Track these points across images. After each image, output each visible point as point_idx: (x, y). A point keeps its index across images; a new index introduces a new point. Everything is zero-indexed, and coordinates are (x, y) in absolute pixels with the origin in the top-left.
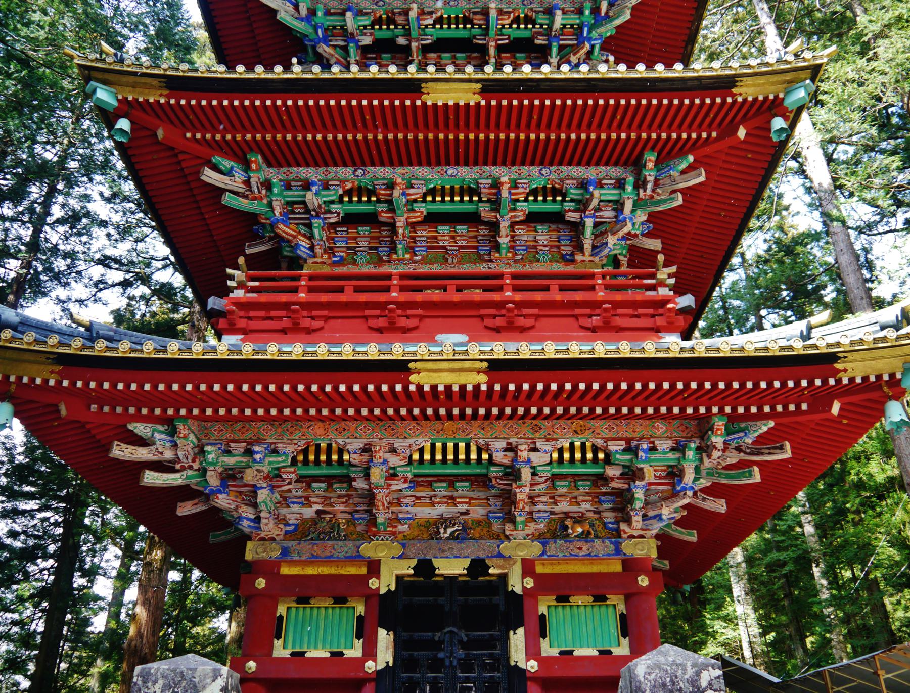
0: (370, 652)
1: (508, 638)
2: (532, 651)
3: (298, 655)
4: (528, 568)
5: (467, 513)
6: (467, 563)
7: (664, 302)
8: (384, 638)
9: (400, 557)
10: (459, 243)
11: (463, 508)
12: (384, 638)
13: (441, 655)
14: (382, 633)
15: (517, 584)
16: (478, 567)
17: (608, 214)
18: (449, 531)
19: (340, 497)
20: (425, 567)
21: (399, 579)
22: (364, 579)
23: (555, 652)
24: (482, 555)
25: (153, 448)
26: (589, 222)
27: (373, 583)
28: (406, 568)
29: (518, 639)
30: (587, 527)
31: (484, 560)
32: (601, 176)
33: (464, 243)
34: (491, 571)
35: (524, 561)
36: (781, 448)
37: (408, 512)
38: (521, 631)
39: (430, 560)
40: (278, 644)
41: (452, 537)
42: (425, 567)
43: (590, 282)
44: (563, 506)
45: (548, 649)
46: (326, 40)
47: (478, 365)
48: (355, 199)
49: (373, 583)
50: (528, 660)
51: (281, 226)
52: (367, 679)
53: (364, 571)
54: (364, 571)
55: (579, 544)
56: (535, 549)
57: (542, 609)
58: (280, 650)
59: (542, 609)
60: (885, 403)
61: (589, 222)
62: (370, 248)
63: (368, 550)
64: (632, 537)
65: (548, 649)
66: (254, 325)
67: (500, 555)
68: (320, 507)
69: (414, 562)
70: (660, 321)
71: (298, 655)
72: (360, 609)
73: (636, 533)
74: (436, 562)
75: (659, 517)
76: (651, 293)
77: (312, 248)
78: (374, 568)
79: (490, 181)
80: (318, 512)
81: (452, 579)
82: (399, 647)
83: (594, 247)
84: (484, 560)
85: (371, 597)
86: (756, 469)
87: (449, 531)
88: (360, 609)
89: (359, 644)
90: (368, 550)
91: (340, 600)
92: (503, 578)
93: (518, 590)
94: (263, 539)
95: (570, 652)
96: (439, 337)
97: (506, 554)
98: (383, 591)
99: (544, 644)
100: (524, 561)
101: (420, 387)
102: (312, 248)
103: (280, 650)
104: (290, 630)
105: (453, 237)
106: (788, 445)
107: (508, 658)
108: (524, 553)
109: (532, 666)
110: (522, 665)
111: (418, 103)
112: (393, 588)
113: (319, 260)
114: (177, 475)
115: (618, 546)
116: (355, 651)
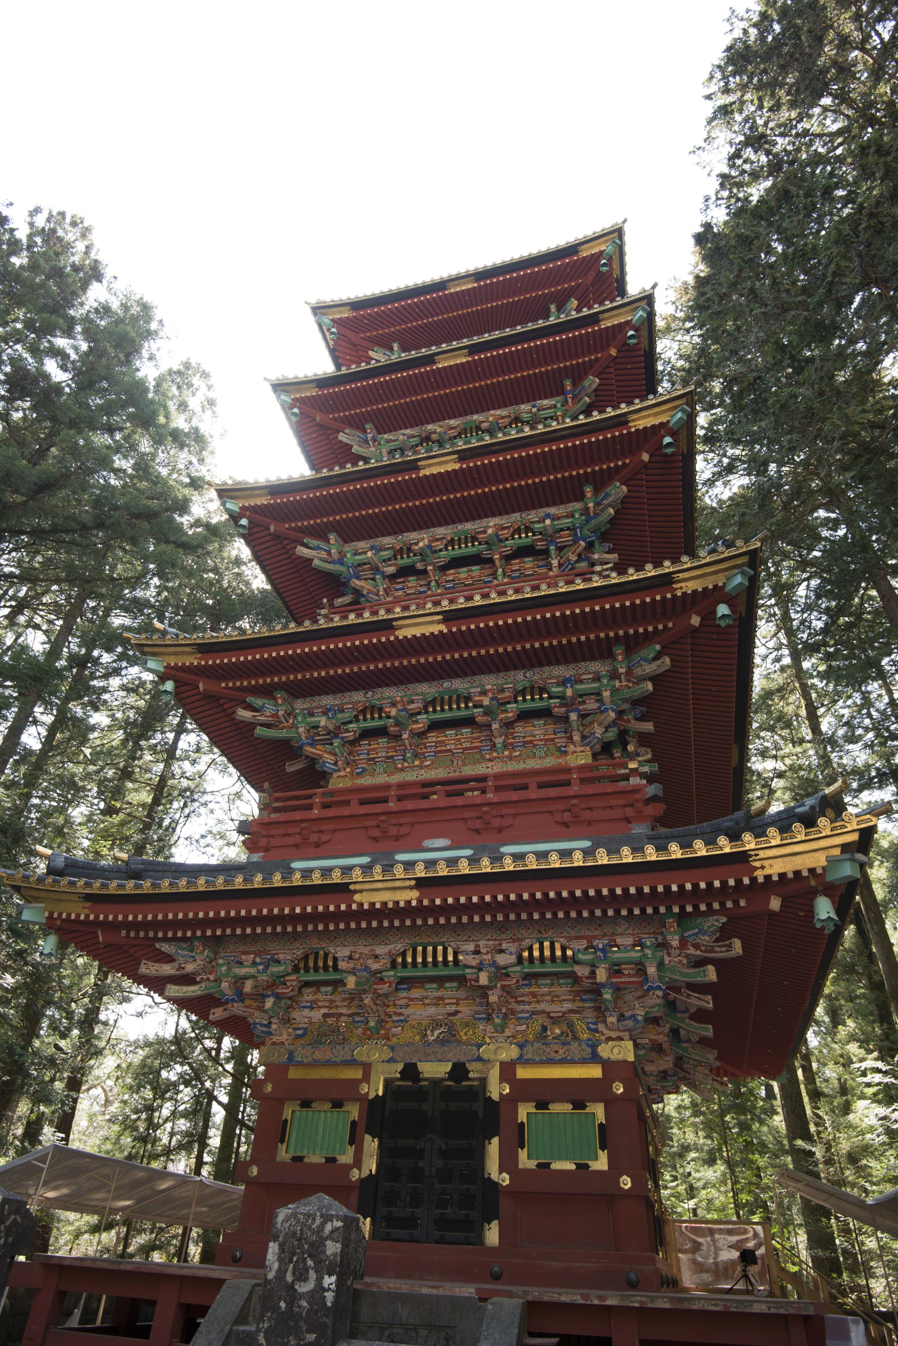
1: (484, 1148)
2: (508, 1162)
4: (507, 1071)
5: (456, 1013)
6: (448, 1067)
7: (636, 790)
8: (371, 1145)
9: (391, 1060)
10: (464, 745)
13: (421, 1164)
14: (368, 1138)
15: (496, 1089)
16: (459, 1071)
18: (436, 1033)
19: (344, 1000)
20: (410, 1071)
21: (388, 1083)
22: (356, 1083)
23: (532, 1164)
24: (462, 1059)
25: (176, 964)
29: (494, 1147)
30: (565, 1028)
31: (464, 1064)
32: (580, 671)
33: (469, 745)
34: (471, 1075)
35: (502, 1064)
36: (730, 946)
37: (401, 1014)
38: (495, 1141)
39: (415, 1064)
40: (282, 1148)
42: (410, 1071)
43: (567, 777)
45: (525, 1160)
47: (407, 883)
48: (369, 716)
49: (364, 1088)
50: (500, 1173)
51: (309, 749)
55: (556, 1047)
59: (522, 1117)
60: (813, 900)
62: (388, 758)
63: (361, 1053)
64: (610, 1039)
65: (525, 1160)
66: (274, 842)
67: (479, 1059)
68: (326, 1011)
69: (400, 1067)
70: (629, 812)
73: (614, 1034)
74: (422, 1067)
75: (633, 1017)
76: (622, 784)
77: (336, 764)
79: (479, 689)
80: (325, 1016)
81: (435, 1082)
82: (383, 1154)
83: (584, 737)
84: (464, 1064)
86: (711, 969)
87: (436, 1033)
89: (351, 1150)
91: (337, 1104)
92: (483, 1081)
93: (495, 1096)
94: (274, 1043)
95: (548, 1165)
96: (427, 843)
97: (485, 1057)
98: (372, 1096)
99: (523, 1154)
100: (502, 1064)
101: (361, 905)
102: (336, 764)
104: (293, 1136)
105: (459, 740)
106: (737, 944)
107: (483, 1170)
108: (504, 1056)
109: (505, 1179)
110: (494, 1176)
111: (392, 638)
112: (380, 1094)
113: (342, 773)
114: (196, 988)
115: (594, 1047)
116: (346, 1158)
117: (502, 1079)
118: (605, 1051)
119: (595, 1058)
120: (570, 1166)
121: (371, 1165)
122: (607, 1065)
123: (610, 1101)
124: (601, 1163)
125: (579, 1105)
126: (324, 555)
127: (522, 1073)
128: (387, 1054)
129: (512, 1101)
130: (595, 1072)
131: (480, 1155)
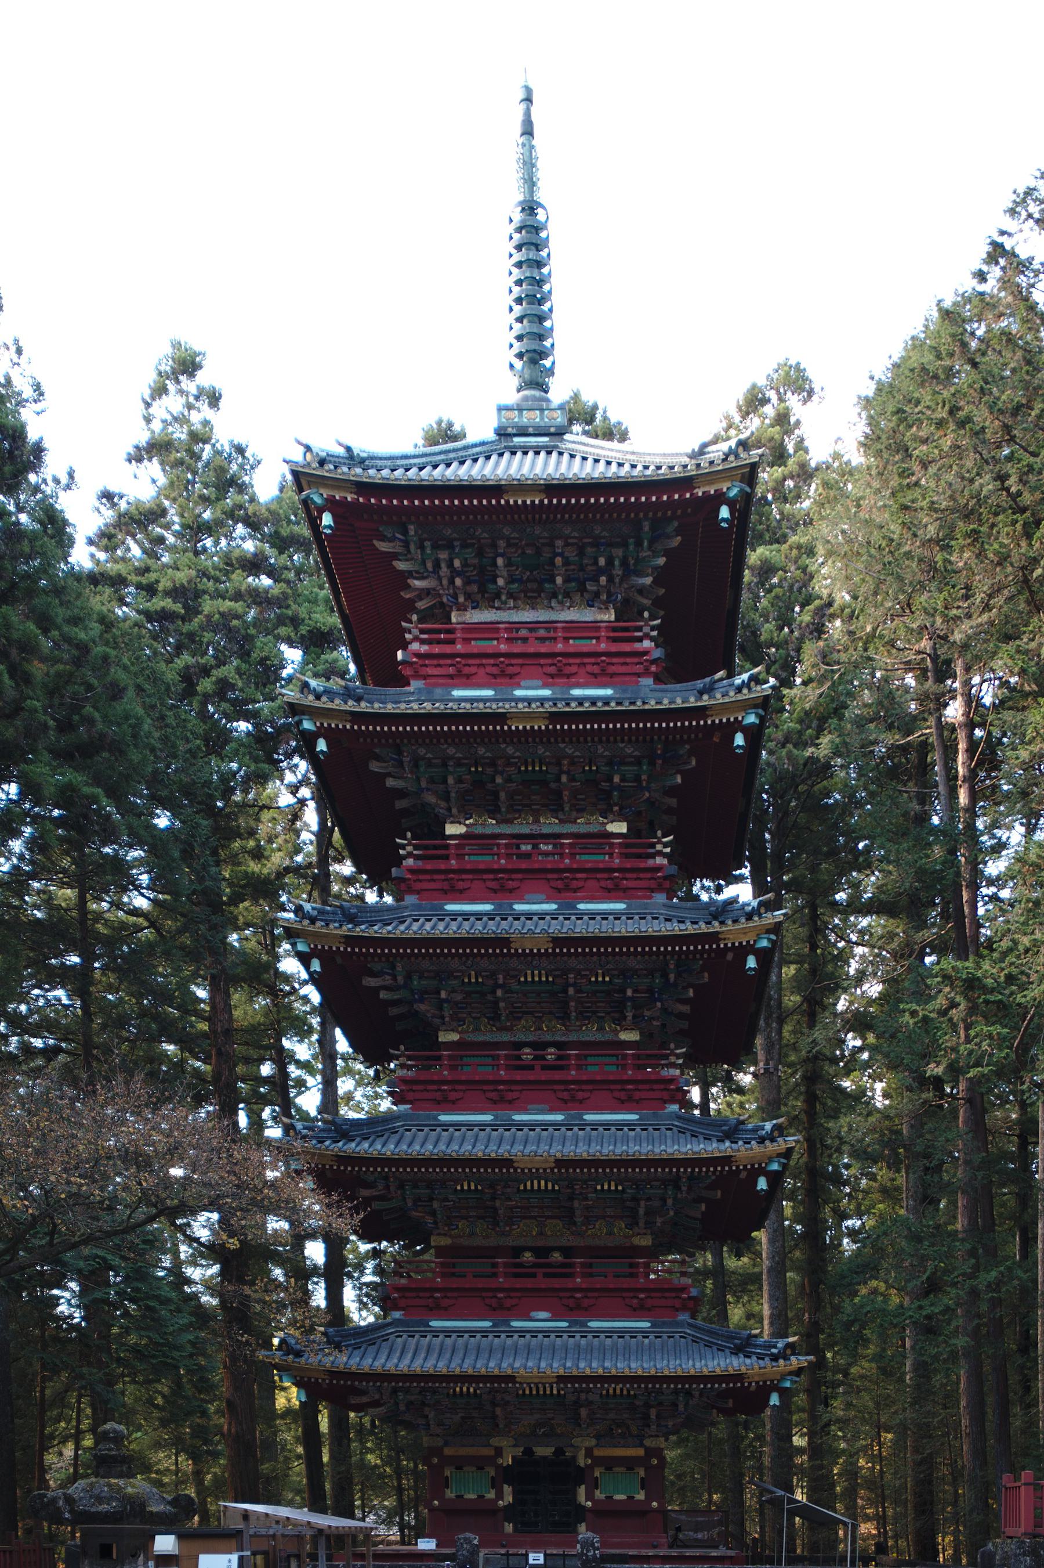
0: (500, 1496)
2: (589, 1496)
3: (460, 1497)
4: (589, 1452)
8: (507, 1489)
9: (515, 1446)
11: (550, 1416)
12: (507, 1489)
14: (506, 1487)
15: (582, 1462)
16: (559, 1452)
17: (656, 1203)
20: (529, 1452)
21: (513, 1458)
23: (603, 1496)
26: (641, 1211)
27: (499, 1461)
28: (519, 1451)
29: (582, 1491)
41: (545, 1434)
42: (529, 1452)
44: (612, 1415)
45: (599, 1495)
46: (421, 1001)
49: (499, 1461)
52: (499, 1510)
53: (492, 1453)
54: (492, 1453)
56: (594, 1442)
57: (597, 1474)
58: (450, 1494)
59: (597, 1474)
61: (641, 1211)
65: (599, 1495)
71: (460, 1497)
72: (492, 1473)
78: (499, 1452)
81: (545, 1458)
85: (498, 1467)
88: (492, 1473)
90: (495, 1441)
92: (574, 1458)
93: (582, 1465)
99: (597, 1493)
103: (450, 1494)
108: (587, 1444)
116: (491, 1495)
117: (586, 1456)
118: (647, 1442)
119: (641, 1445)
120: (623, 1497)
121: (509, 1498)
122: (647, 1450)
123: (648, 1468)
124: (641, 1496)
125: (630, 1469)
126: (388, 980)
127: (597, 1452)
128: (512, 1442)
129: (590, 1468)
130: (641, 1452)
131: (575, 1494)
